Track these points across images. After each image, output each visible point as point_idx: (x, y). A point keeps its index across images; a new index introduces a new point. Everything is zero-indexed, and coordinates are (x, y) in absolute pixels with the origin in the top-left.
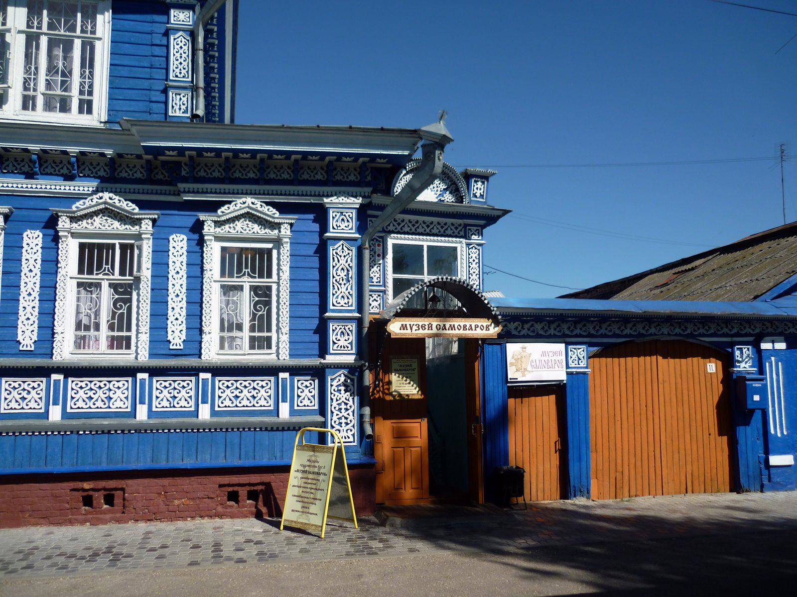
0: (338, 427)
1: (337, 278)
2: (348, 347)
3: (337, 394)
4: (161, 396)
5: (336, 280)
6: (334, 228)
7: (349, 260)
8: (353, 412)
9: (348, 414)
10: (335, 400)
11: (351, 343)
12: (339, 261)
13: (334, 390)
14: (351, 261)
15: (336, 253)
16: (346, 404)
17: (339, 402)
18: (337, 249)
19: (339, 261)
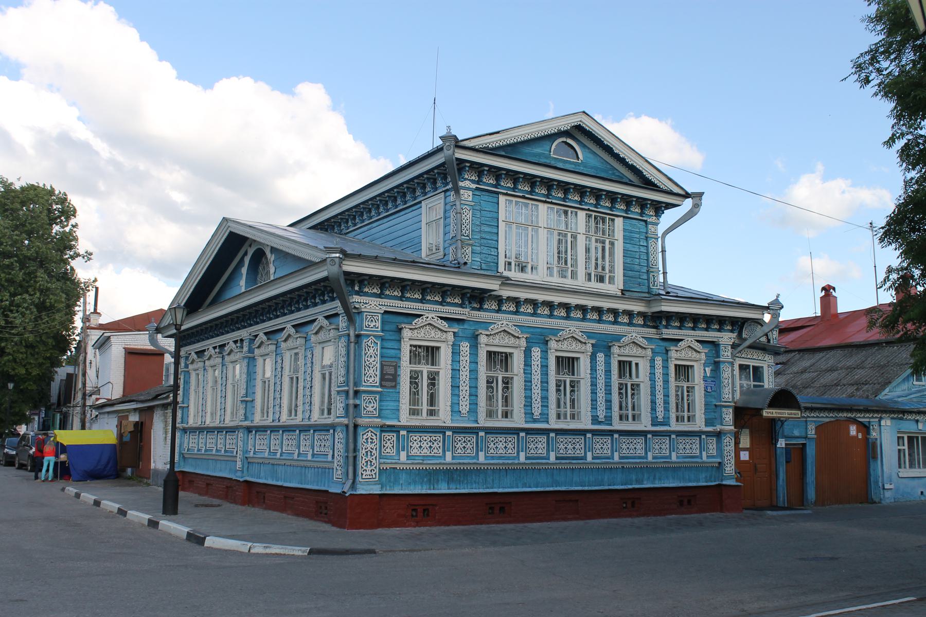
1: (367, 363)
6: (366, 327)
8: (376, 458)
18: (368, 341)
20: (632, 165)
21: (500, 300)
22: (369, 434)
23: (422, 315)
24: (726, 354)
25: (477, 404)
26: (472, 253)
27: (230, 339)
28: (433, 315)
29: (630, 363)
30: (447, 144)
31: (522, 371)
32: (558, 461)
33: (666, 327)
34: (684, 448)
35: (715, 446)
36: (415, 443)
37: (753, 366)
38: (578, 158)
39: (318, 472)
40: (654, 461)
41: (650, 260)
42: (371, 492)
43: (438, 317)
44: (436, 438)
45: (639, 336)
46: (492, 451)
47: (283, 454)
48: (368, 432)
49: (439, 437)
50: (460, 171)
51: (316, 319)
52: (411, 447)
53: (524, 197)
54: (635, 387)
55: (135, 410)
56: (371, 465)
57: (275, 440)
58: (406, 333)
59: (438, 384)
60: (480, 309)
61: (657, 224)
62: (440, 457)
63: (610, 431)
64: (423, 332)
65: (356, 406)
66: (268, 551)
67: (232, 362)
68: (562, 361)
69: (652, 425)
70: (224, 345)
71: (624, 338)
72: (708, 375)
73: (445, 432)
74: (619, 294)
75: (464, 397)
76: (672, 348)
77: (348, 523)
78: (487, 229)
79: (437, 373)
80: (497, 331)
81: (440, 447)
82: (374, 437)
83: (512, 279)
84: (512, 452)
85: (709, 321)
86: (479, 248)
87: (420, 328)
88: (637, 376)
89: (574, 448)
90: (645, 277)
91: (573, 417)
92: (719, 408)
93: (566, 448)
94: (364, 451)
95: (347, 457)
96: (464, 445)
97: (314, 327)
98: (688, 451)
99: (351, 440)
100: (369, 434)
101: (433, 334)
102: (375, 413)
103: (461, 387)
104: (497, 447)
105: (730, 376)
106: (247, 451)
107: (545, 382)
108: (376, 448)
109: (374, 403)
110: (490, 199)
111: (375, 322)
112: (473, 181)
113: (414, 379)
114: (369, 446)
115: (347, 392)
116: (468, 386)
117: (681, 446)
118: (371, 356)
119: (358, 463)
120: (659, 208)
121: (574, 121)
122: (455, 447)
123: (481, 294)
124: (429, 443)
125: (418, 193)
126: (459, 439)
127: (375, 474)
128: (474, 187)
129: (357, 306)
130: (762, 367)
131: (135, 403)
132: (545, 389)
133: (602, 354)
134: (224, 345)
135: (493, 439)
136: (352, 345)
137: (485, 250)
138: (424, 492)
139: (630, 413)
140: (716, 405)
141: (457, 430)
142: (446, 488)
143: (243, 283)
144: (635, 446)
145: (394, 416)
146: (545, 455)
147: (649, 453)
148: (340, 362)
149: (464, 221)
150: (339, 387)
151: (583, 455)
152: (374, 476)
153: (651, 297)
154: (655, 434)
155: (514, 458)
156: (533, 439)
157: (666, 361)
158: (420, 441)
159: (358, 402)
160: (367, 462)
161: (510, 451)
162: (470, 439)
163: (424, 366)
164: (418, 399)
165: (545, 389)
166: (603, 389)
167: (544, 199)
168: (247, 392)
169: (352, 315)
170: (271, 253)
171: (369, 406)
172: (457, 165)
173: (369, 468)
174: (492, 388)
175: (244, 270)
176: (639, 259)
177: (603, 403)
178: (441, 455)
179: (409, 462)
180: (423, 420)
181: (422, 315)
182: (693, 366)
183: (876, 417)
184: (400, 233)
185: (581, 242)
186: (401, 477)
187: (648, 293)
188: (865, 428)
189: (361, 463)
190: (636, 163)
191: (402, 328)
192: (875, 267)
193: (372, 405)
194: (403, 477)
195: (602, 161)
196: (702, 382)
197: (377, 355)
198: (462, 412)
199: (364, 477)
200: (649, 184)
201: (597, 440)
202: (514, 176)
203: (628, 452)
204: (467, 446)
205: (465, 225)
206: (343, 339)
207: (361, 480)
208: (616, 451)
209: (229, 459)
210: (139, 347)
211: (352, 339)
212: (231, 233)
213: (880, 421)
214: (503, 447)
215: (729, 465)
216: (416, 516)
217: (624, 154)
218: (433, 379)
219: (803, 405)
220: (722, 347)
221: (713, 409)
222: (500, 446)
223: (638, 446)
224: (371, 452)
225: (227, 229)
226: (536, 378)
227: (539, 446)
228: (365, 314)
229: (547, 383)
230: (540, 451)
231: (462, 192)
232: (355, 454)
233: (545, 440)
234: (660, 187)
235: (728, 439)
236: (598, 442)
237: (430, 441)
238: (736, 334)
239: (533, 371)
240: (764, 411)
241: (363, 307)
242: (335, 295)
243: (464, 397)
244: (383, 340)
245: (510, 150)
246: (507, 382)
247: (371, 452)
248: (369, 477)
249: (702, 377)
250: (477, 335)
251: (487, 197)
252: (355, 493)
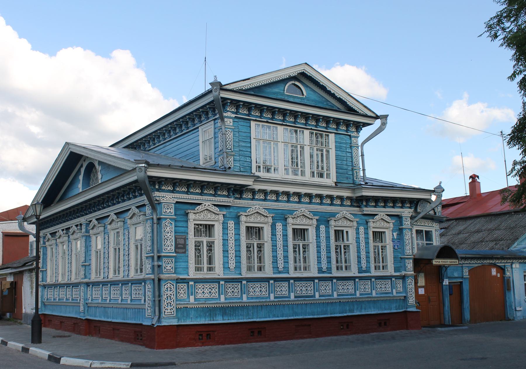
1: (166, 237)
6: (164, 213)
7: (171, 228)
8: (174, 300)
9: (171, 302)
11: (172, 268)
15: (165, 225)
18: (166, 223)
20: (340, 98)
21: (253, 192)
22: (169, 285)
23: (201, 204)
24: (407, 223)
25: (240, 262)
26: (234, 160)
27: (73, 224)
28: (209, 204)
29: (342, 231)
30: (215, 88)
31: (270, 239)
32: (296, 299)
33: (366, 206)
34: (381, 287)
35: (401, 285)
36: (200, 290)
37: (425, 231)
38: (303, 95)
39: (135, 311)
40: (361, 296)
41: (354, 161)
42: (171, 324)
43: (212, 204)
44: (214, 286)
45: (348, 213)
46: (252, 294)
47: (111, 300)
48: (168, 283)
49: (216, 285)
50: (224, 105)
51: (130, 209)
52: (197, 292)
53: (267, 122)
54: (347, 247)
55: (11, 273)
56: (171, 306)
57: (105, 291)
58: (191, 216)
59: (214, 249)
60: (241, 198)
61: (357, 137)
62: (217, 299)
63: (331, 277)
64: (202, 215)
65: (159, 266)
66: (103, 366)
67: (74, 239)
68: (297, 231)
69: (359, 272)
70: (69, 228)
71: (338, 215)
72: (395, 238)
73: (220, 282)
74: (334, 185)
75: (232, 258)
76: (370, 220)
77: (156, 345)
78: (244, 144)
79: (213, 242)
80: (252, 213)
81: (216, 292)
82: (172, 287)
83: (262, 177)
84: (265, 294)
85: (394, 200)
86: (238, 157)
87: (200, 212)
88: (348, 240)
89: (307, 290)
90: (351, 173)
91: (305, 269)
92: (403, 260)
93: (301, 290)
94: (165, 296)
95: (154, 300)
96: (233, 290)
97: (130, 214)
98: (383, 289)
99: (156, 289)
100: (169, 285)
101: (209, 216)
102: (172, 270)
103: (229, 251)
104: (255, 291)
105: (410, 238)
106: (87, 299)
107: (285, 246)
108: (174, 294)
109: (171, 264)
110: (245, 124)
111: (170, 209)
112: (233, 113)
113: (198, 246)
114: (169, 293)
115: (153, 257)
116: (234, 250)
117: (378, 286)
118: (168, 232)
119: (162, 304)
120: (359, 126)
121: (300, 69)
122: (227, 292)
123: (241, 188)
124: (209, 289)
125: (196, 122)
126: (230, 286)
127: (174, 311)
128: (234, 116)
129: (158, 199)
130: (431, 231)
131: (11, 269)
132: (286, 251)
133: (324, 226)
134: (69, 228)
135: (252, 285)
136: (155, 225)
137: (242, 159)
138: (206, 322)
139: (344, 265)
140: (401, 258)
141: (227, 280)
142: (222, 319)
143: (80, 186)
144: (348, 287)
145: (185, 272)
146: (287, 295)
147: (357, 291)
148: (147, 237)
149: (228, 139)
150: (147, 254)
151: (313, 294)
152: (173, 313)
153: (355, 186)
154: (361, 278)
155: (267, 298)
156: (279, 285)
157: (366, 229)
158: (203, 288)
159: (160, 263)
160: (168, 304)
161: (264, 293)
162: (236, 286)
163: (204, 238)
164: (201, 260)
165: (286, 251)
166: (325, 250)
167: (281, 123)
168: (85, 259)
169: (154, 205)
170: (99, 165)
171: (168, 266)
172: (222, 101)
173: (169, 308)
174: (250, 251)
175: (81, 177)
176: (346, 161)
177: (325, 259)
178: (217, 297)
179: (196, 302)
180: (205, 274)
181: (201, 204)
182: (385, 232)
183: (509, 263)
184: (185, 149)
185: (307, 150)
186: (191, 313)
187: (353, 184)
188: (502, 270)
189: (164, 304)
190: (342, 96)
191: (189, 213)
192: (505, 161)
193: (170, 265)
194: (192, 313)
195: (319, 96)
196: (391, 242)
197: (172, 231)
198: (231, 268)
199: (166, 314)
200: (351, 110)
201: (322, 284)
202: (260, 108)
203: (343, 291)
204: (235, 291)
205: (229, 142)
206: (149, 222)
207: (164, 316)
208: (335, 291)
209: (75, 304)
210: (12, 231)
211: (155, 221)
212: (72, 153)
213: (512, 265)
214: (259, 290)
215: (411, 298)
216: (202, 339)
217: (334, 91)
218: (210, 246)
219: (459, 256)
220: (404, 219)
221: (399, 261)
222: (257, 290)
223: (349, 287)
224: (170, 297)
225: (69, 150)
226: (280, 243)
227: (283, 289)
228: (163, 204)
229: (287, 246)
230: (284, 293)
231: (226, 120)
232: (159, 299)
233: (287, 285)
234: (358, 112)
235: (410, 280)
236: (323, 285)
237: (210, 288)
238: (413, 210)
239: (278, 239)
240: (434, 261)
241: (161, 199)
242: (143, 192)
243: (232, 258)
244: (176, 221)
245: (257, 91)
246: (260, 247)
247: (170, 297)
248: (169, 314)
249: (391, 239)
250: (239, 216)
251: (243, 123)
252: (160, 325)
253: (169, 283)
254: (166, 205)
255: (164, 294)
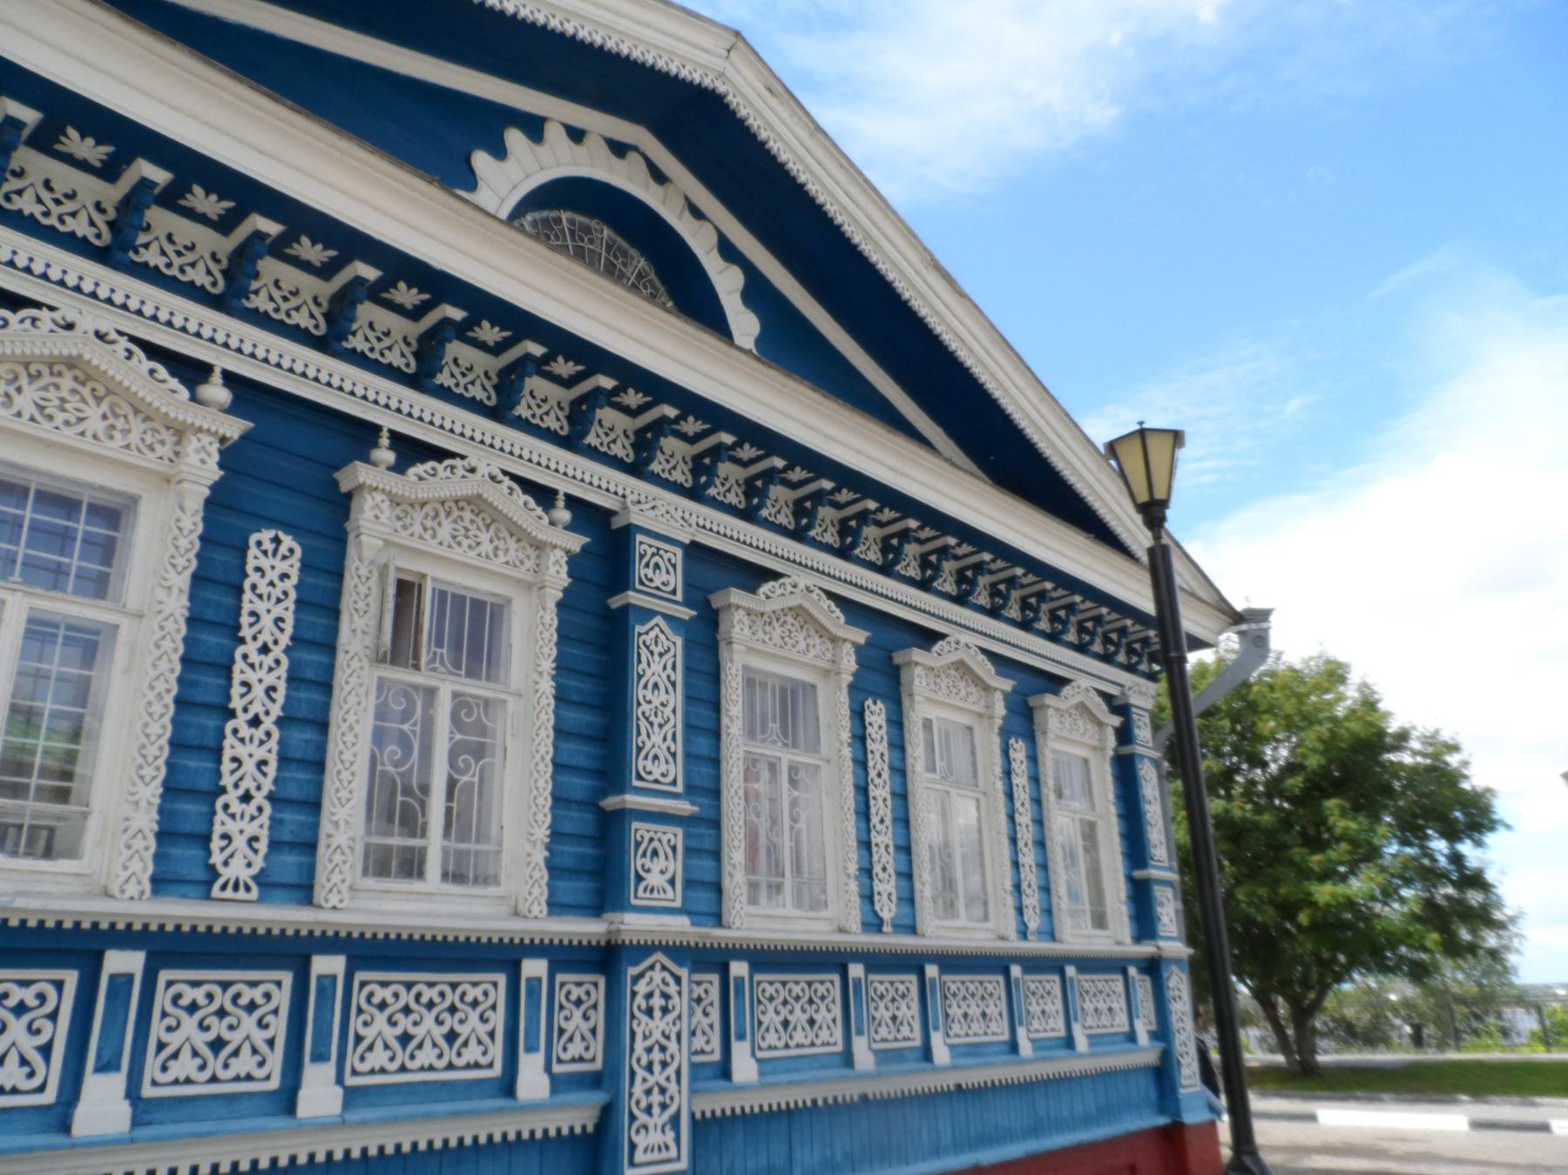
0: (642, 1117)
2: (664, 891)
3: (644, 1018)
4: (174, 1040)
5: (643, 713)
8: (678, 1073)
10: (639, 1037)
12: (649, 664)
13: (639, 1008)
14: (674, 668)
15: (644, 642)
16: (663, 1049)
17: (649, 1043)
18: (647, 633)
19: (649, 664)
22: (657, 975)
43: (820, 589)
48: (652, 967)
82: (672, 989)
100: (657, 975)
114: (658, 1024)
118: (656, 686)
199: (639, 1156)
247: (663, 1049)
248: (656, 1156)
253: (658, 967)
254: (651, 546)
255: (633, 1034)
